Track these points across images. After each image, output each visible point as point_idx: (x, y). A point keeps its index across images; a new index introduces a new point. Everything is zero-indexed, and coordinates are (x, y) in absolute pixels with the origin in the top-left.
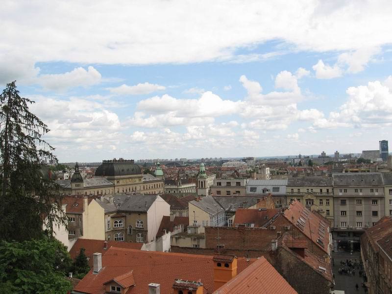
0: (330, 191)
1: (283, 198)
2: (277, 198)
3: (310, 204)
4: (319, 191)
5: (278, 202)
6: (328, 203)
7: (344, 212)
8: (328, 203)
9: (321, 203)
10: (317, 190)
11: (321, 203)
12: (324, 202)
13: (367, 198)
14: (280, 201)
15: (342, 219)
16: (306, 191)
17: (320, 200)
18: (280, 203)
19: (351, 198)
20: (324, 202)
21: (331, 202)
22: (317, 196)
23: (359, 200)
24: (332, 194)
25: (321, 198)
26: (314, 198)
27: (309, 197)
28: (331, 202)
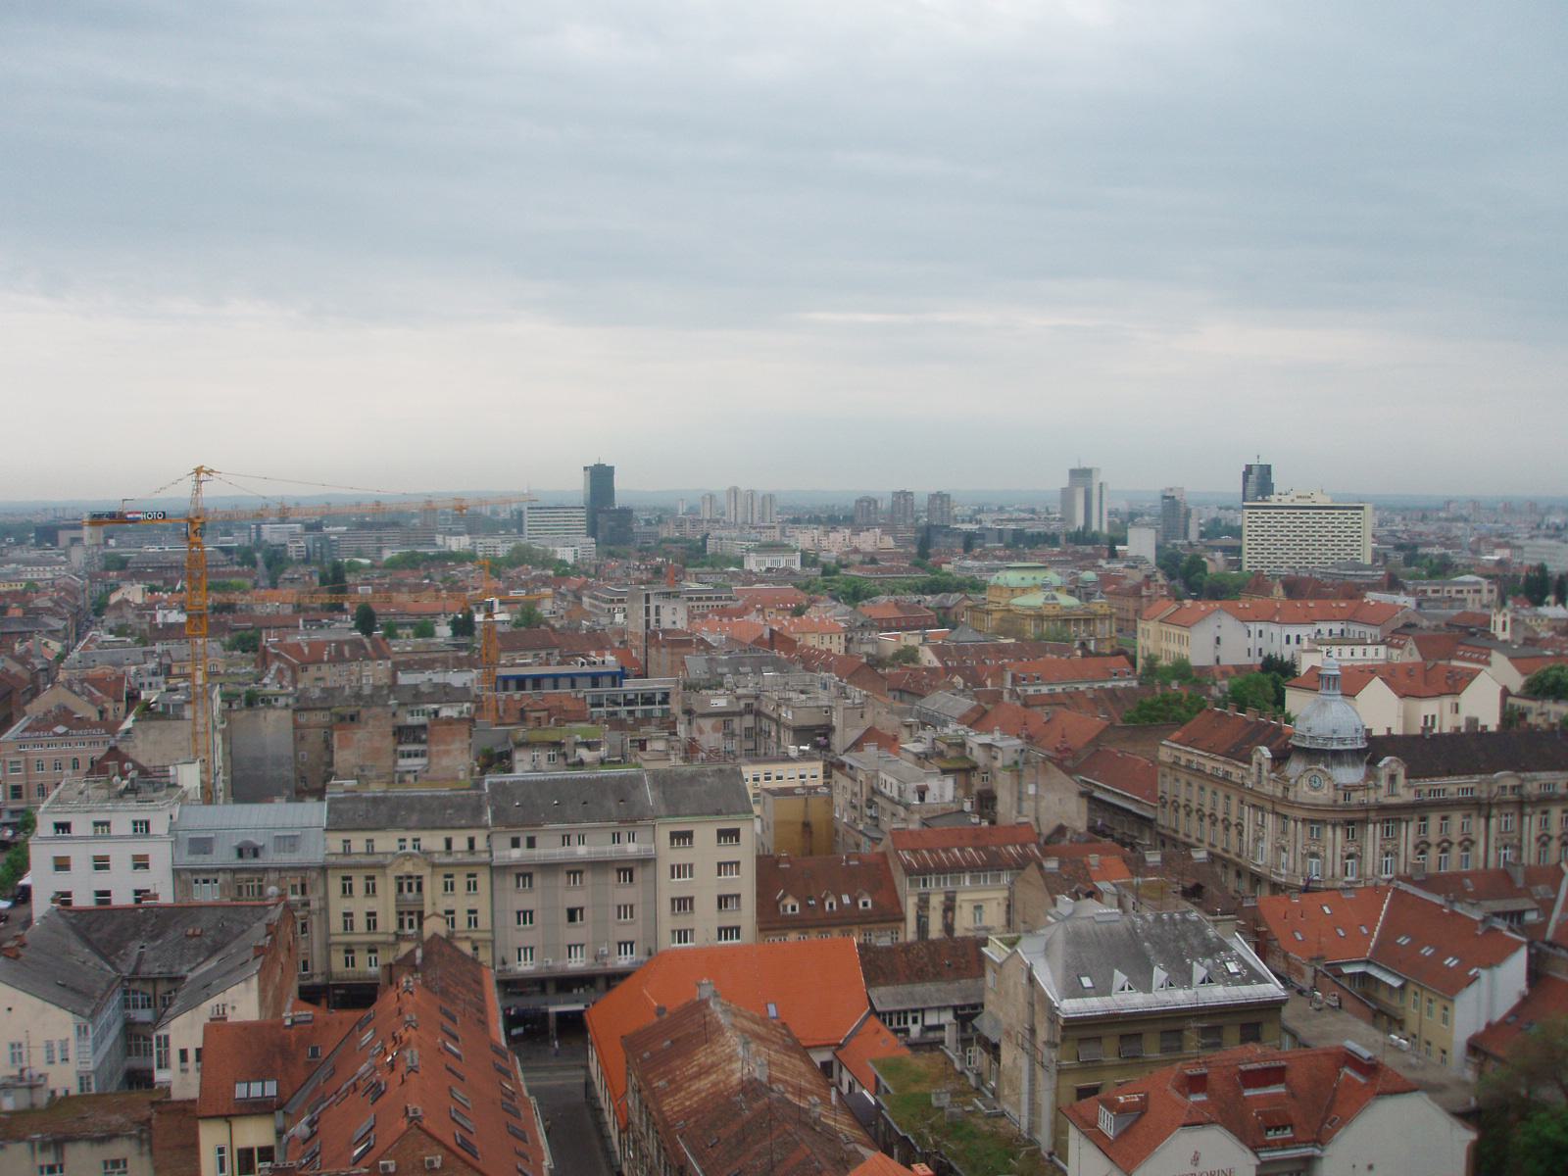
0: (480, 843)
1: (314, 875)
2: (291, 874)
3: (410, 890)
4: (442, 846)
5: (294, 887)
6: (472, 887)
7: (525, 913)
8: (472, 887)
9: (449, 887)
10: (433, 841)
11: (449, 887)
12: (460, 882)
13: (598, 865)
14: (303, 886)
15: (526, 936)
16: (394, 846)
17: (447, 876)
18: (304, 892)
19: (550, 868)
20: (460, 882)
21: (483, 880)
22: (434, 866)
23: (575, 870)
24: (485, 857)
25: (449, 871)
26: (426, 872)
27: (409, 868)
28: (483, 880)
